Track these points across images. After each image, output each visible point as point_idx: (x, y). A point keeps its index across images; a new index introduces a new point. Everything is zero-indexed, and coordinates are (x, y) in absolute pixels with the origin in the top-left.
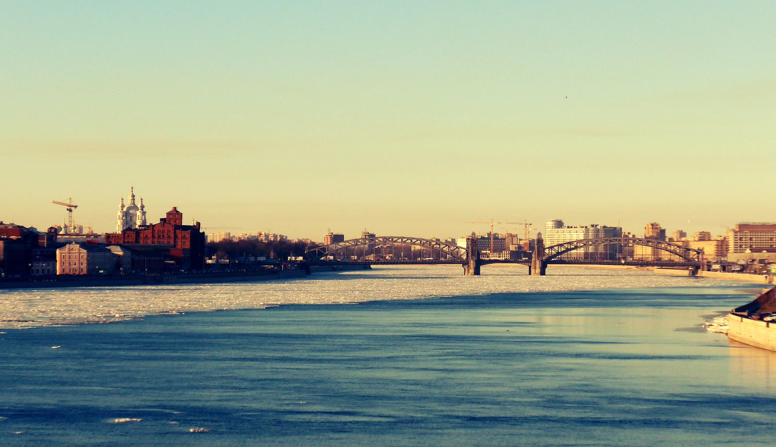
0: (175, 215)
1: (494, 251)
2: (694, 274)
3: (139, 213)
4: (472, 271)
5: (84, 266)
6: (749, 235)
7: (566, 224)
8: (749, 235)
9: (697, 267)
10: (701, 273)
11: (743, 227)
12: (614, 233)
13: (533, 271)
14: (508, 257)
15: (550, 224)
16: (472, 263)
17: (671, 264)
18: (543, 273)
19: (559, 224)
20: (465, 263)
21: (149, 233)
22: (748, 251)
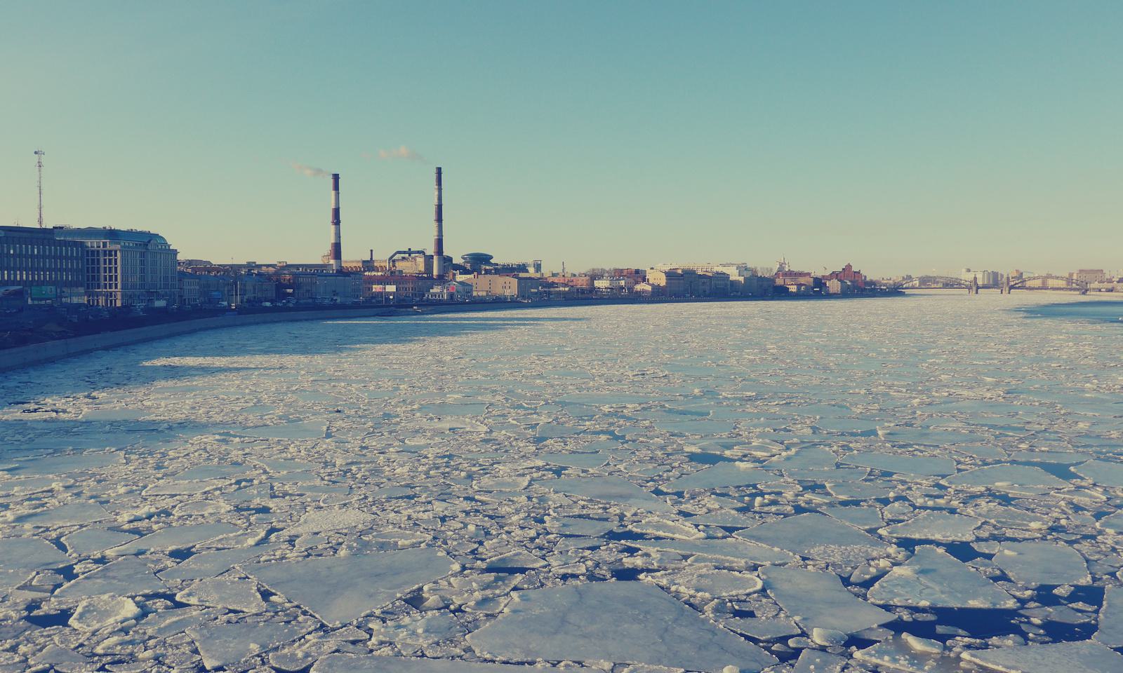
0: (849, 266)
1: (934, 283)
2: (1084, 293)
3: (787, 266)
4: (974, 292)
5: (839, 289)
6: (1085, 275)
7: (972, 270)
8: (1085, 275)
9: (1087, 290)
10: (1088, 293)
11: (1081, 271)
12: (995, 275)
13: (1004, 292)
14: (941, 286)
15: (964, 270)
16: (974, 288)
17: (1075, 289)
18: (1009, 293)
19: (969, 270)
20: (969, 288)
21: (842, 274)
22: (1097, 283)
